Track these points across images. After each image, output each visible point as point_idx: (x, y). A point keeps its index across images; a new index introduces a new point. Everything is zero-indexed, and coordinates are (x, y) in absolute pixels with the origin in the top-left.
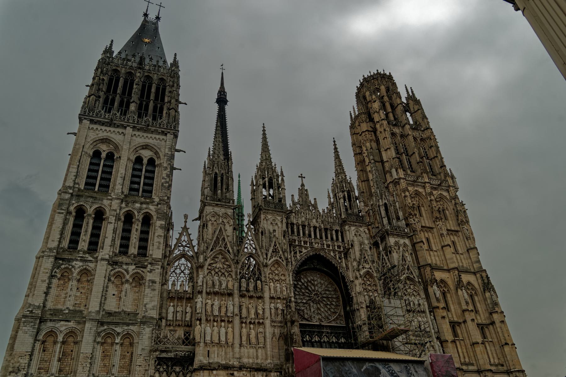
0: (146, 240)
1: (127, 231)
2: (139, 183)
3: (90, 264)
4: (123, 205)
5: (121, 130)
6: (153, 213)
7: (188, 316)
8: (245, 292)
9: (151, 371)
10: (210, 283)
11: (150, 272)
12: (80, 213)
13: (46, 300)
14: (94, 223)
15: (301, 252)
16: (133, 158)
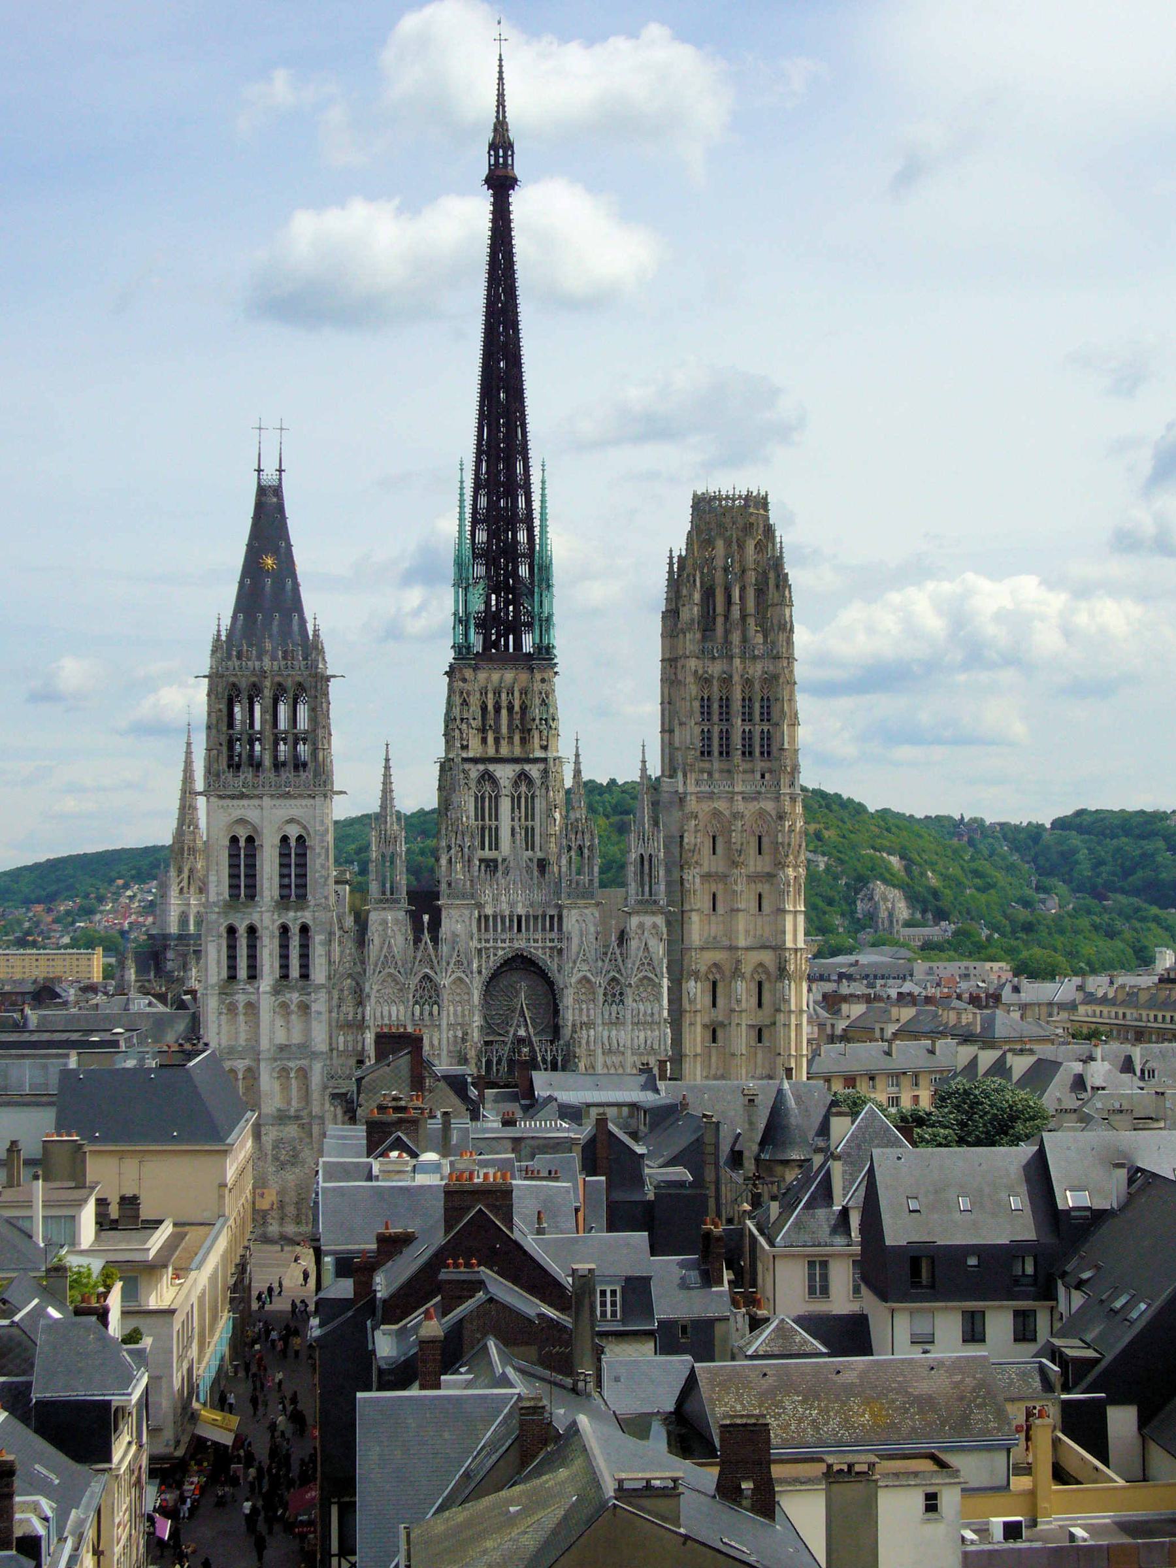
0: (307, 956)
1: (284, 946)
2: (290, 876)
3: (252, 996)
4: (276, 917)
5: (256, 802)
6: (310, 923)
7: (360, 1045)
8: (419, 1022)
9: (327, 1105)
10: (378, 1014)
11: (314, 1002)
12: (232, 931)
13: (220, 1039)
14: (248, 941)
15: (495, 955)
16: (277, 841)
